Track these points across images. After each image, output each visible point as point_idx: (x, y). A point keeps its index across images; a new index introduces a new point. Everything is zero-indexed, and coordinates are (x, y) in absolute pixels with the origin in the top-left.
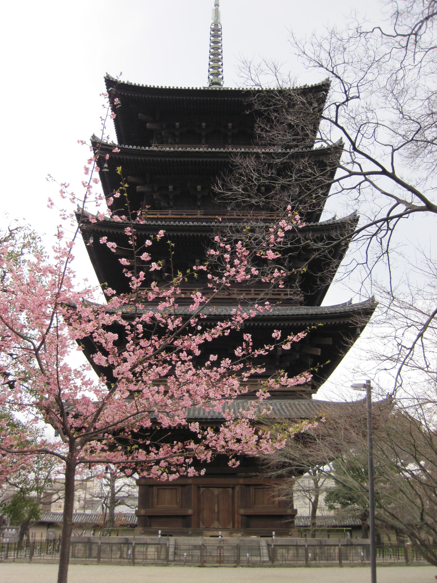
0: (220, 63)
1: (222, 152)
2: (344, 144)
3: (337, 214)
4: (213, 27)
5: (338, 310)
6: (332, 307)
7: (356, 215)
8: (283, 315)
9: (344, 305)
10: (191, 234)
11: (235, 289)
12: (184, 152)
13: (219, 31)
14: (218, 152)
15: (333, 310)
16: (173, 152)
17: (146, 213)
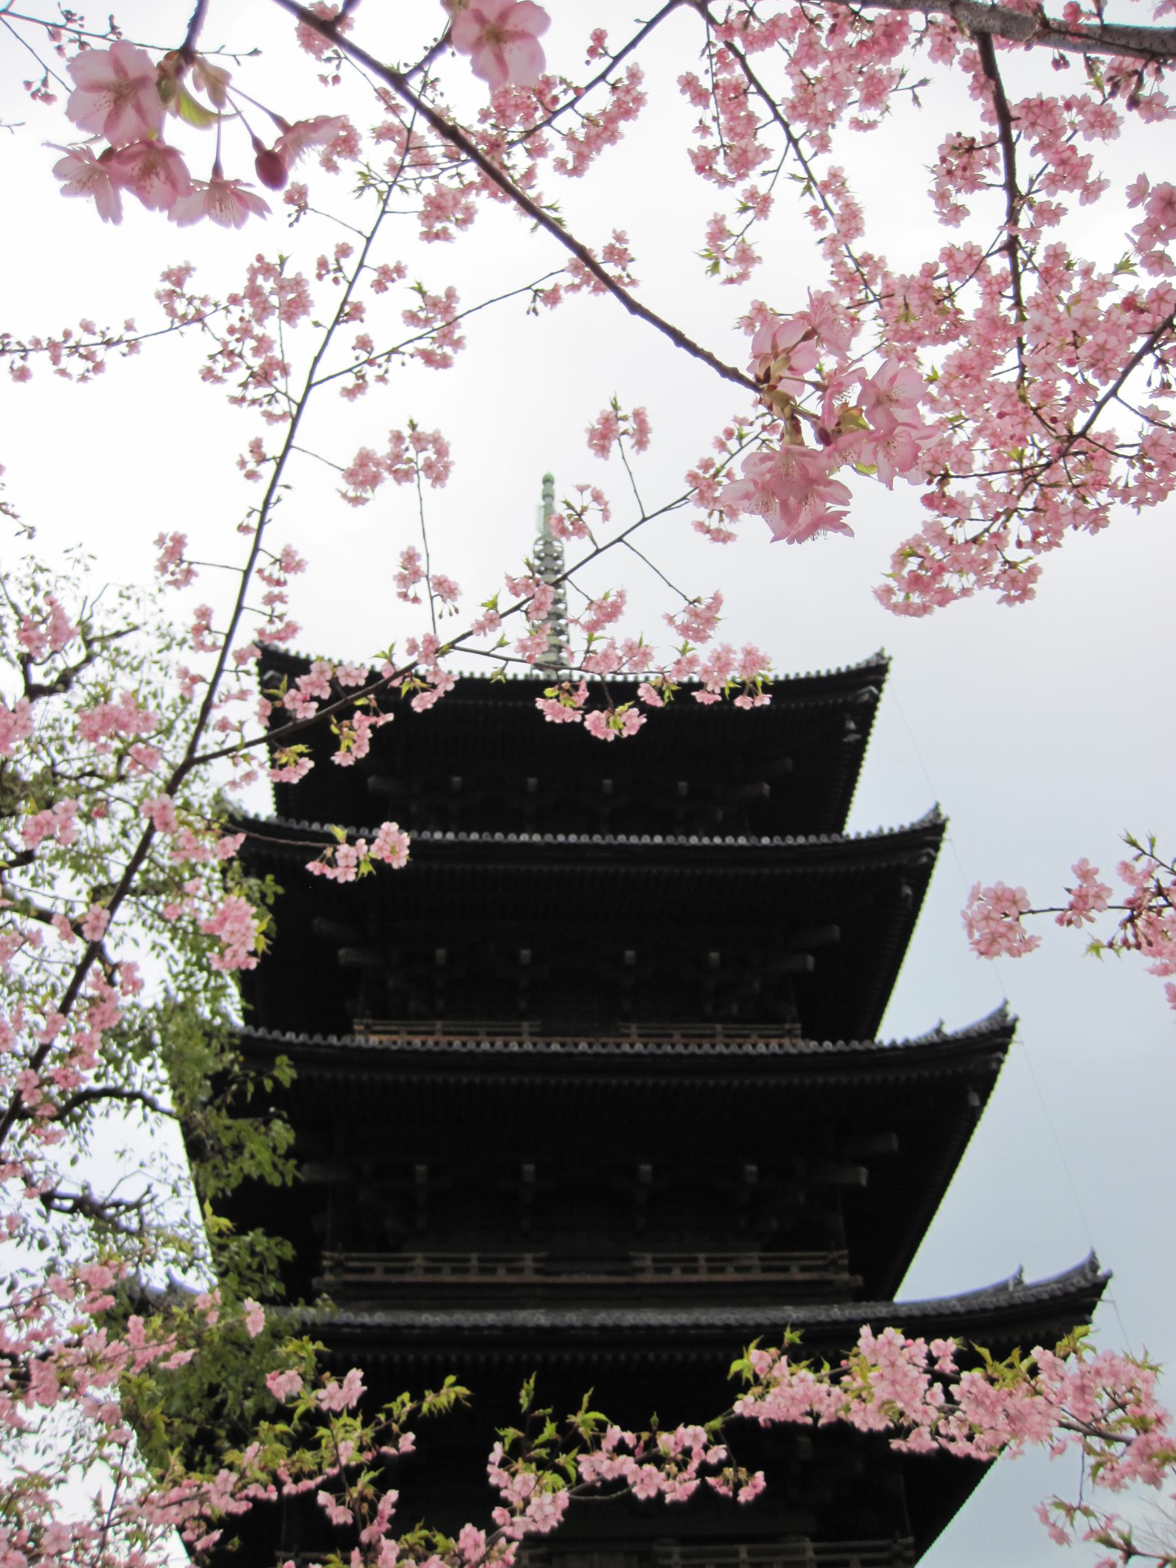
0: (563, 638)
1: (597, 846)
2: (946, 820)
3: (946, 1020)
4: (539, 548)
5: (991, 1302)
6: (961, 1299)
7: (1006, 1015)
8: (820, 1323)
9: (1002, 1288)
10: (514, 1080)
11: (649, 1256)
12: (486, 844)
13: (557, 558)
14: (585, 846)
15: (975, 1305)
16: (451, 845)
17: (368, 1027)
